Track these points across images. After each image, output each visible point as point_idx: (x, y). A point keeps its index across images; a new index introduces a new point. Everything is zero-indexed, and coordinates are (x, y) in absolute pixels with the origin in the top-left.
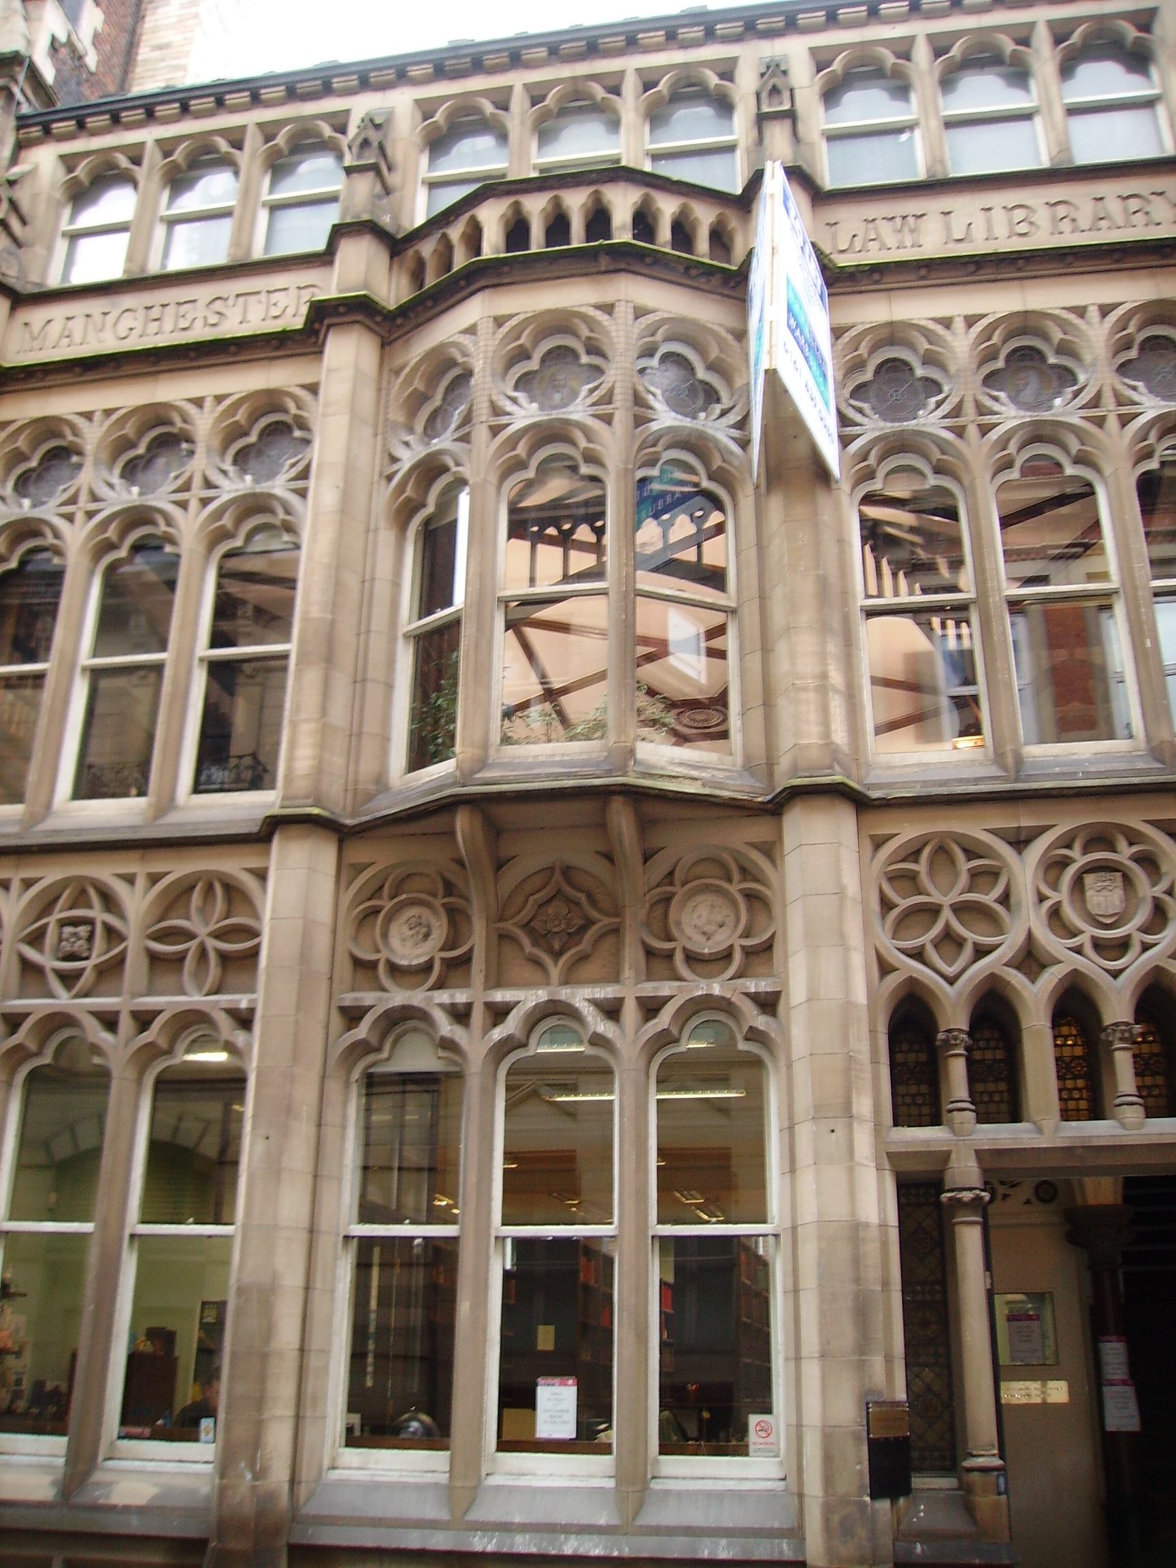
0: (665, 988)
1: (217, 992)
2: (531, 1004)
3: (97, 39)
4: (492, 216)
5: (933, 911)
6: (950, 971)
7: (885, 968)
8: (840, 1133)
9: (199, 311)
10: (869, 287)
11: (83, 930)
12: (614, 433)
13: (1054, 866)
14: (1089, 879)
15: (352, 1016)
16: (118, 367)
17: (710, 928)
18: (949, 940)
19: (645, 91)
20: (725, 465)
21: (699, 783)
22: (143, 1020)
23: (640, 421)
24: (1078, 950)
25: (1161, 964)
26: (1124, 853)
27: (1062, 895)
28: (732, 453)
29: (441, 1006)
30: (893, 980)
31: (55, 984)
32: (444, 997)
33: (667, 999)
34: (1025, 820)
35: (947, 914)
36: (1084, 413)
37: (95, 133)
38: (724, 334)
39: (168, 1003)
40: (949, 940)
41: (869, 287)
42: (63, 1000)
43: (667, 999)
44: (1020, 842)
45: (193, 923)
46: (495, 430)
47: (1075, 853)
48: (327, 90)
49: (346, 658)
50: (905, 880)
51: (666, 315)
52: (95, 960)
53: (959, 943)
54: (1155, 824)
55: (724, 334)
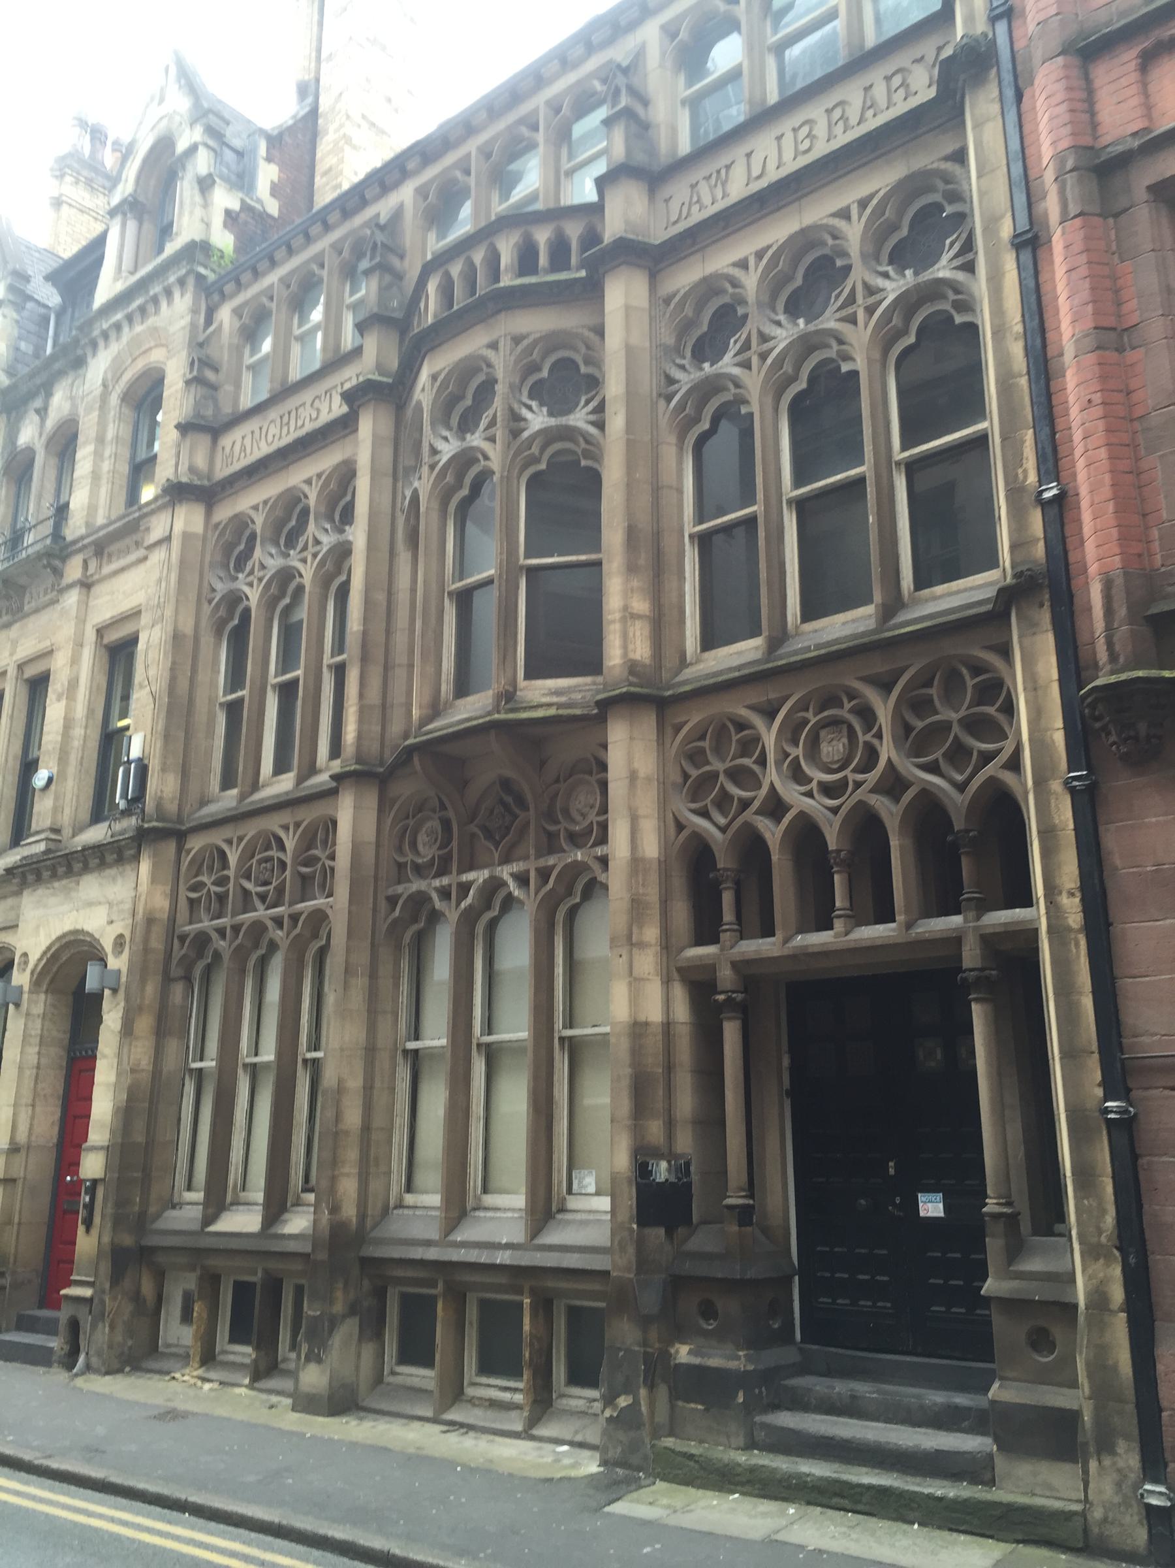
0: (551, 861)
1: (218, 918)
2: (481, 880)
3: (275, 190)
4: (507, 248)
5: (946, 726)
6: (959, 778)
7: (680, 827)
8: (624, 957)
9: (306, 413)
10: (690, 251)
11: (268, 865)
12: (495, 449)
13: (792, 732)
14: (823, 733)
15: (392, 901)
16: (266, 467)
17: (585, 810)
18: (958, 754)
19: (673, 41)
20: (588, 447)
21: (555, 707)
22: (295, 918)
23: (515, 433)
24: (809, 794)
25: (864, 798)
26: (845, 711)
27: (798, 751)
28: (591, 435)
29: (436, 889)
30: (685, 834)
31: (257, 903)
32: (437, 883)
33: (554, 866)
34: (772, 694)
35: (956, 728)
36: (838, 315)
37: (283, 262)
38: (586, 333)
39: (305, 907)
40: (723, 801)
41: (690, 251)
42: (261, 913)
43: (554, 866)
44: (770, 714)
45: (204, 878)
46: (432, 467)
47: (848, 706)
48: (364, 203)
49: (378, 654)
50: (696, 757)
51: (538, 335)
52: (274, 884)
53: (969, 752)
54: (863, 679)
55: (586, 333)
